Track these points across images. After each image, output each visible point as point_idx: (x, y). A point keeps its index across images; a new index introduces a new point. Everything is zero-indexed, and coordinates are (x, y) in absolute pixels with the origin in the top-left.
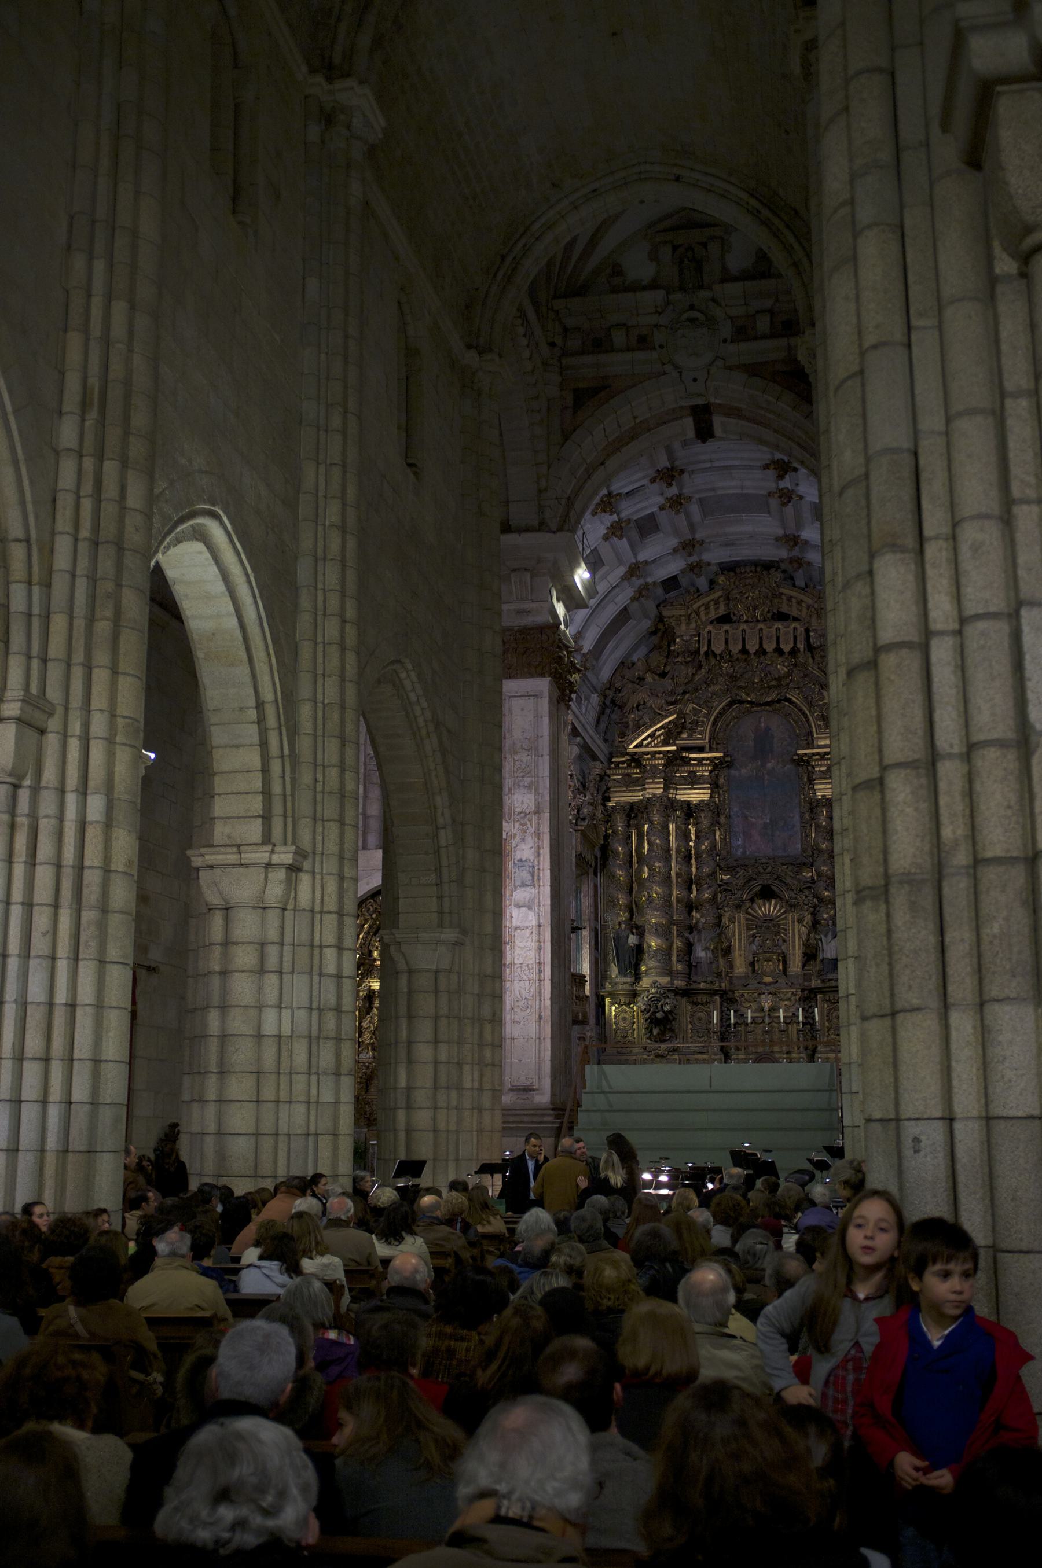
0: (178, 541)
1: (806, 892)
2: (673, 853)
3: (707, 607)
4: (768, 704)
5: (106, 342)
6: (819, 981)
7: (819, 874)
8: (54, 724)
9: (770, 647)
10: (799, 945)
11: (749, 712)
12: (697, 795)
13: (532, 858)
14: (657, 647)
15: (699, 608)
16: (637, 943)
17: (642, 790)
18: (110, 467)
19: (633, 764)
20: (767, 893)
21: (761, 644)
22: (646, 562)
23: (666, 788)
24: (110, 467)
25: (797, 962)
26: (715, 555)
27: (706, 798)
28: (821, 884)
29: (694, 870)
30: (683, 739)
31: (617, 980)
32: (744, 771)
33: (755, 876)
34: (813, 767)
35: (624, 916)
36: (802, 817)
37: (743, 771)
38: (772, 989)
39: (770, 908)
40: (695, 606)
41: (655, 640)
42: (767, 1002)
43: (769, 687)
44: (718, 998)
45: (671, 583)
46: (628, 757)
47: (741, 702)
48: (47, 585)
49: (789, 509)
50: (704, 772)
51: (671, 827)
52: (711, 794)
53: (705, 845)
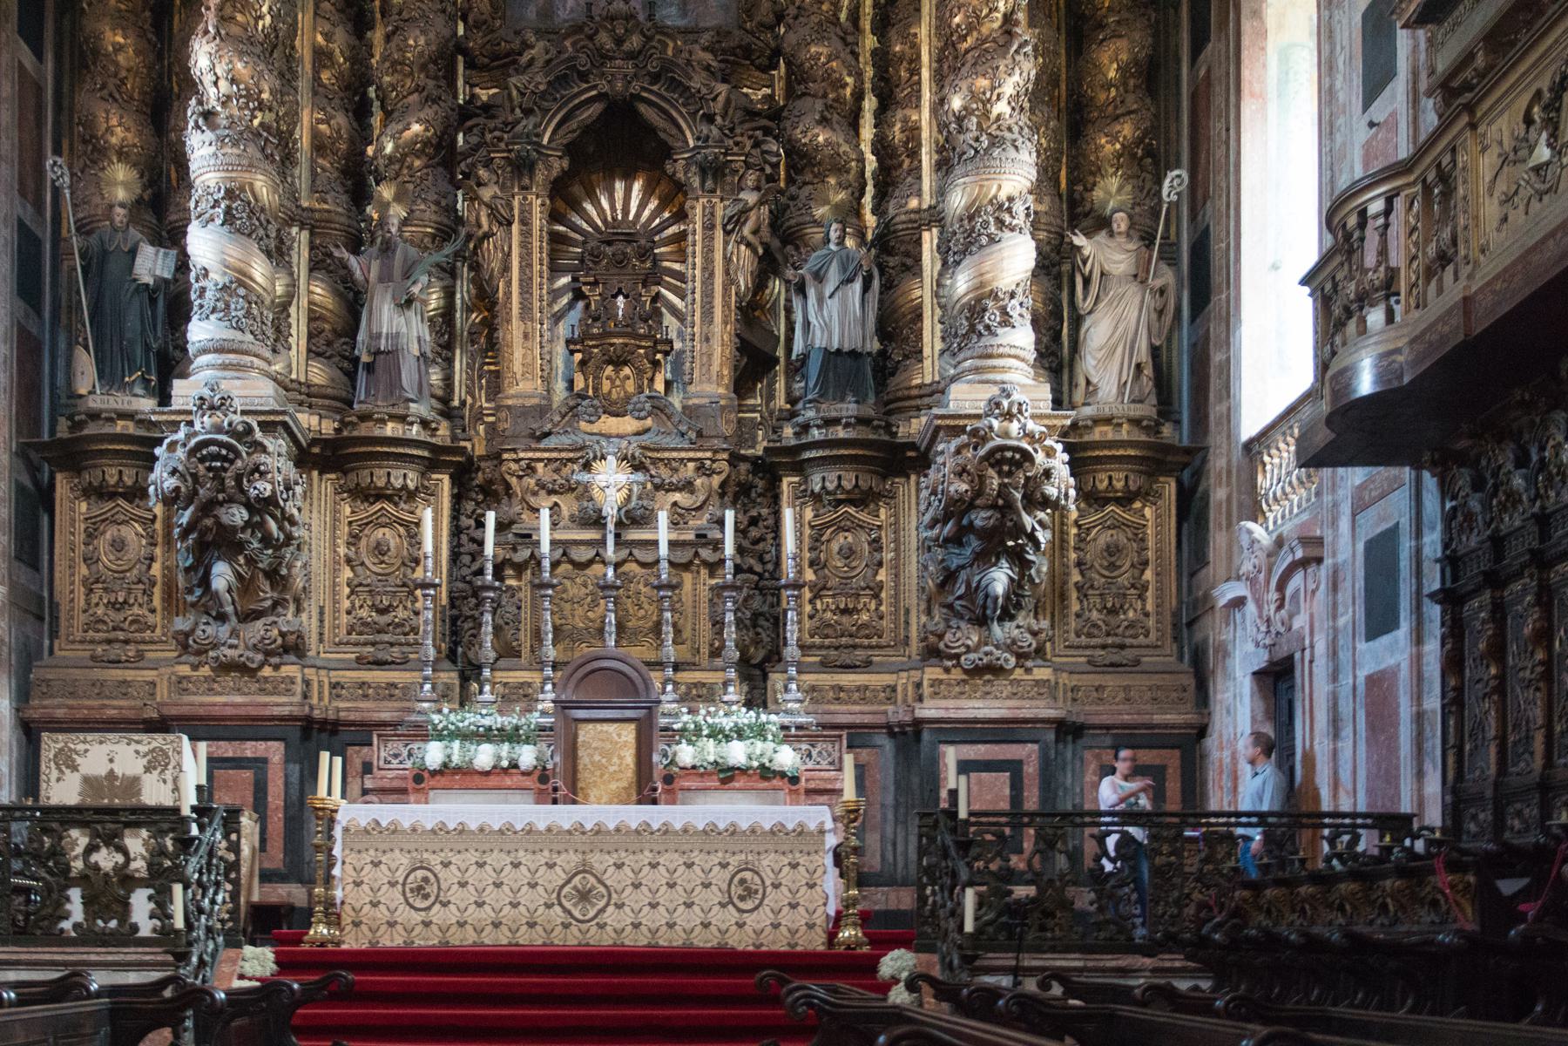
6: (788, 431)
10: (726, 305)
16: (167, 275)
25: (715, 367)
35: (121, 183)
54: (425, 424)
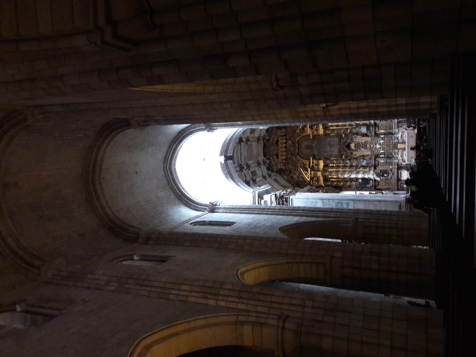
0: (244, 279)
1: (348, 136)
2: (337, 170)
3: (275, 160)
4: (299, 145)
5: (191, 291)
6: (373, 133)
7: (344, 133)
8: (286, 313)
9: (284, 145)
11: (300, 151)
12: (322, 164)
13: (335, 202)
14: (284, 173)
15: (274, 162)
17: (320, 178)
18: (221, 292)
19: (313, 179)
20: (348, 146)
21: (284, 147)
22: (263, 174)
23: (320, 171)
24: (221, 292)
26: (261, 158)
27: (322, 161)
28: (346, 132)
29: (342, 165)
30: (307, 167)
31: (371, 185)
32: (316, 153)
33: (344, 149)
34: (315, 134)
35: (353, 183)
36: (328, 137)
37: (316, 152)
38: (374, 145)
39: (352, 146)
40: (274, 163)
41: (282, 173)
42: (378, 146)
43: (295, 145)
44: (377, 159)
45: (268, 169)
46: (311, 181)
47: (298, 152)
48: (249, 311)
49: (251, 140)
50: (315, 162)
51: (330, 170)
52: (321, 160)
53: (335, 162)
54: (372, 160)
